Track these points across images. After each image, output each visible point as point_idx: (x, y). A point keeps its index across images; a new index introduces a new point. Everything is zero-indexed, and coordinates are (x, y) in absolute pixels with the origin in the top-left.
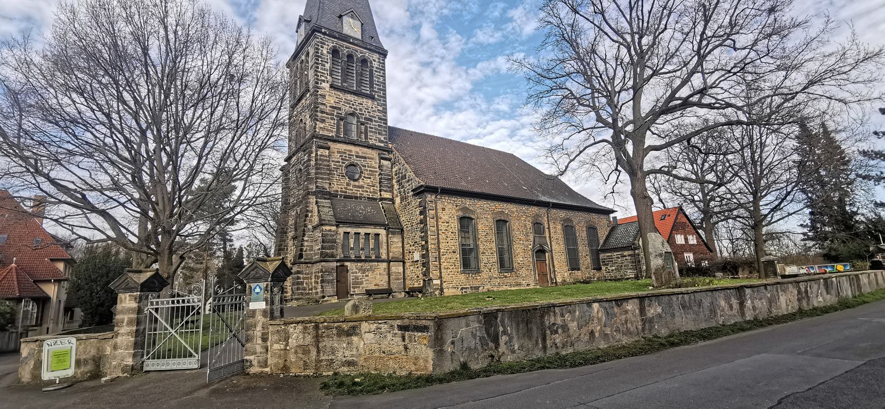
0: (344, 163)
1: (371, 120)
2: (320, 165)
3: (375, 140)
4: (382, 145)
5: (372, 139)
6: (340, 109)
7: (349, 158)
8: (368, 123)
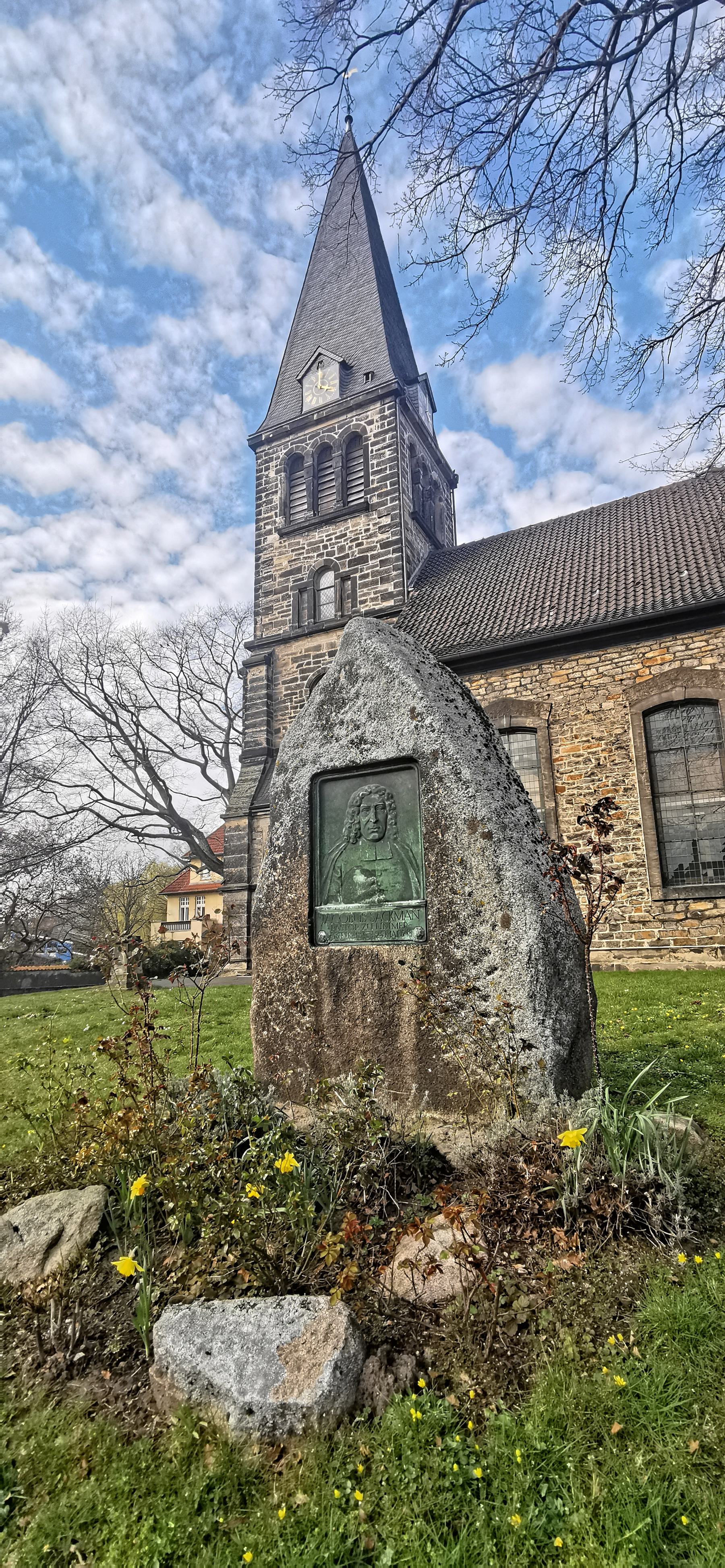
0: (303, 679)
1: (363, 560)
2: (252, 699)
3: (372, 600)
4: (391, 603)
5: (365, 601)
6: (299, 570)
7: (315, 663)
8: (356, 571)
